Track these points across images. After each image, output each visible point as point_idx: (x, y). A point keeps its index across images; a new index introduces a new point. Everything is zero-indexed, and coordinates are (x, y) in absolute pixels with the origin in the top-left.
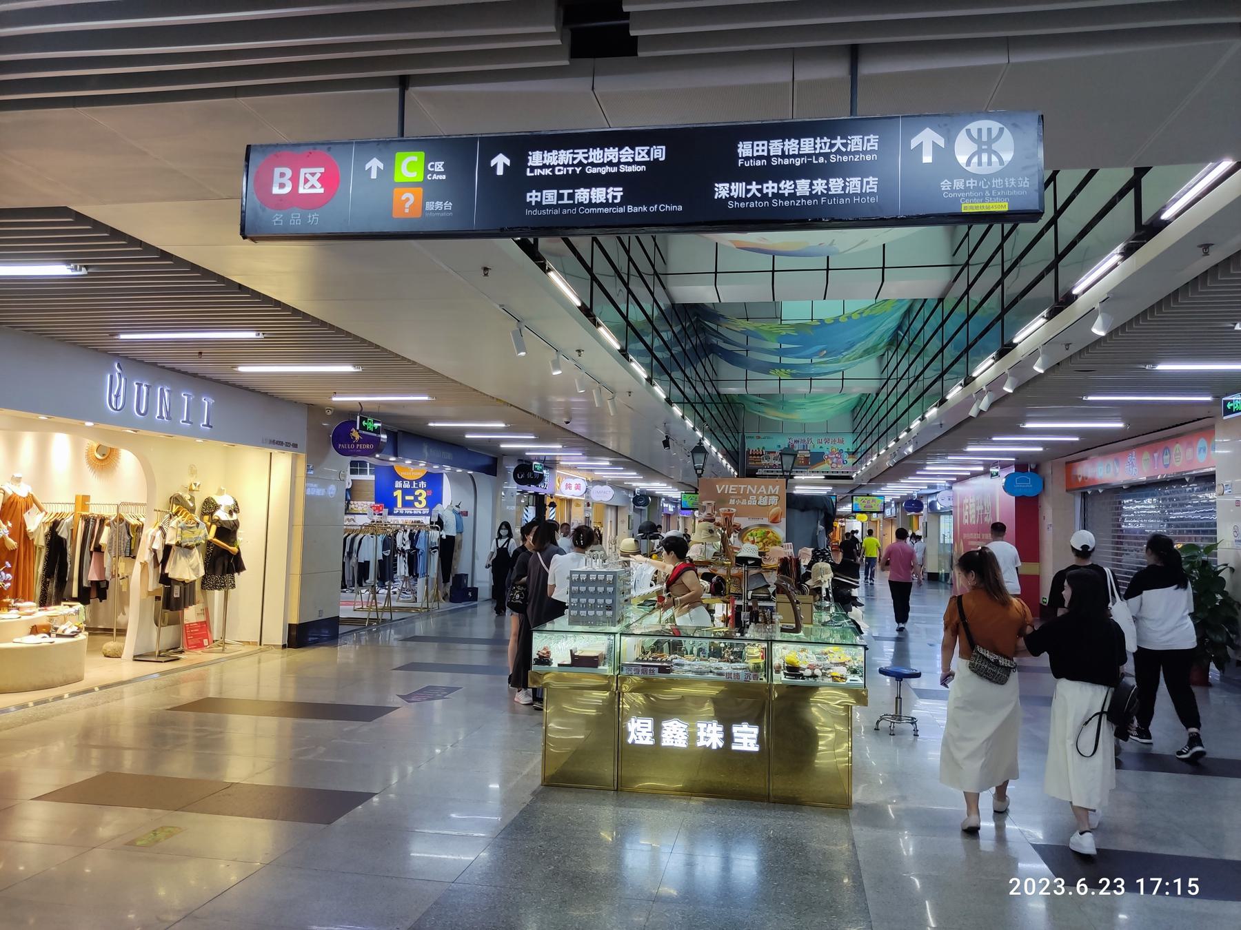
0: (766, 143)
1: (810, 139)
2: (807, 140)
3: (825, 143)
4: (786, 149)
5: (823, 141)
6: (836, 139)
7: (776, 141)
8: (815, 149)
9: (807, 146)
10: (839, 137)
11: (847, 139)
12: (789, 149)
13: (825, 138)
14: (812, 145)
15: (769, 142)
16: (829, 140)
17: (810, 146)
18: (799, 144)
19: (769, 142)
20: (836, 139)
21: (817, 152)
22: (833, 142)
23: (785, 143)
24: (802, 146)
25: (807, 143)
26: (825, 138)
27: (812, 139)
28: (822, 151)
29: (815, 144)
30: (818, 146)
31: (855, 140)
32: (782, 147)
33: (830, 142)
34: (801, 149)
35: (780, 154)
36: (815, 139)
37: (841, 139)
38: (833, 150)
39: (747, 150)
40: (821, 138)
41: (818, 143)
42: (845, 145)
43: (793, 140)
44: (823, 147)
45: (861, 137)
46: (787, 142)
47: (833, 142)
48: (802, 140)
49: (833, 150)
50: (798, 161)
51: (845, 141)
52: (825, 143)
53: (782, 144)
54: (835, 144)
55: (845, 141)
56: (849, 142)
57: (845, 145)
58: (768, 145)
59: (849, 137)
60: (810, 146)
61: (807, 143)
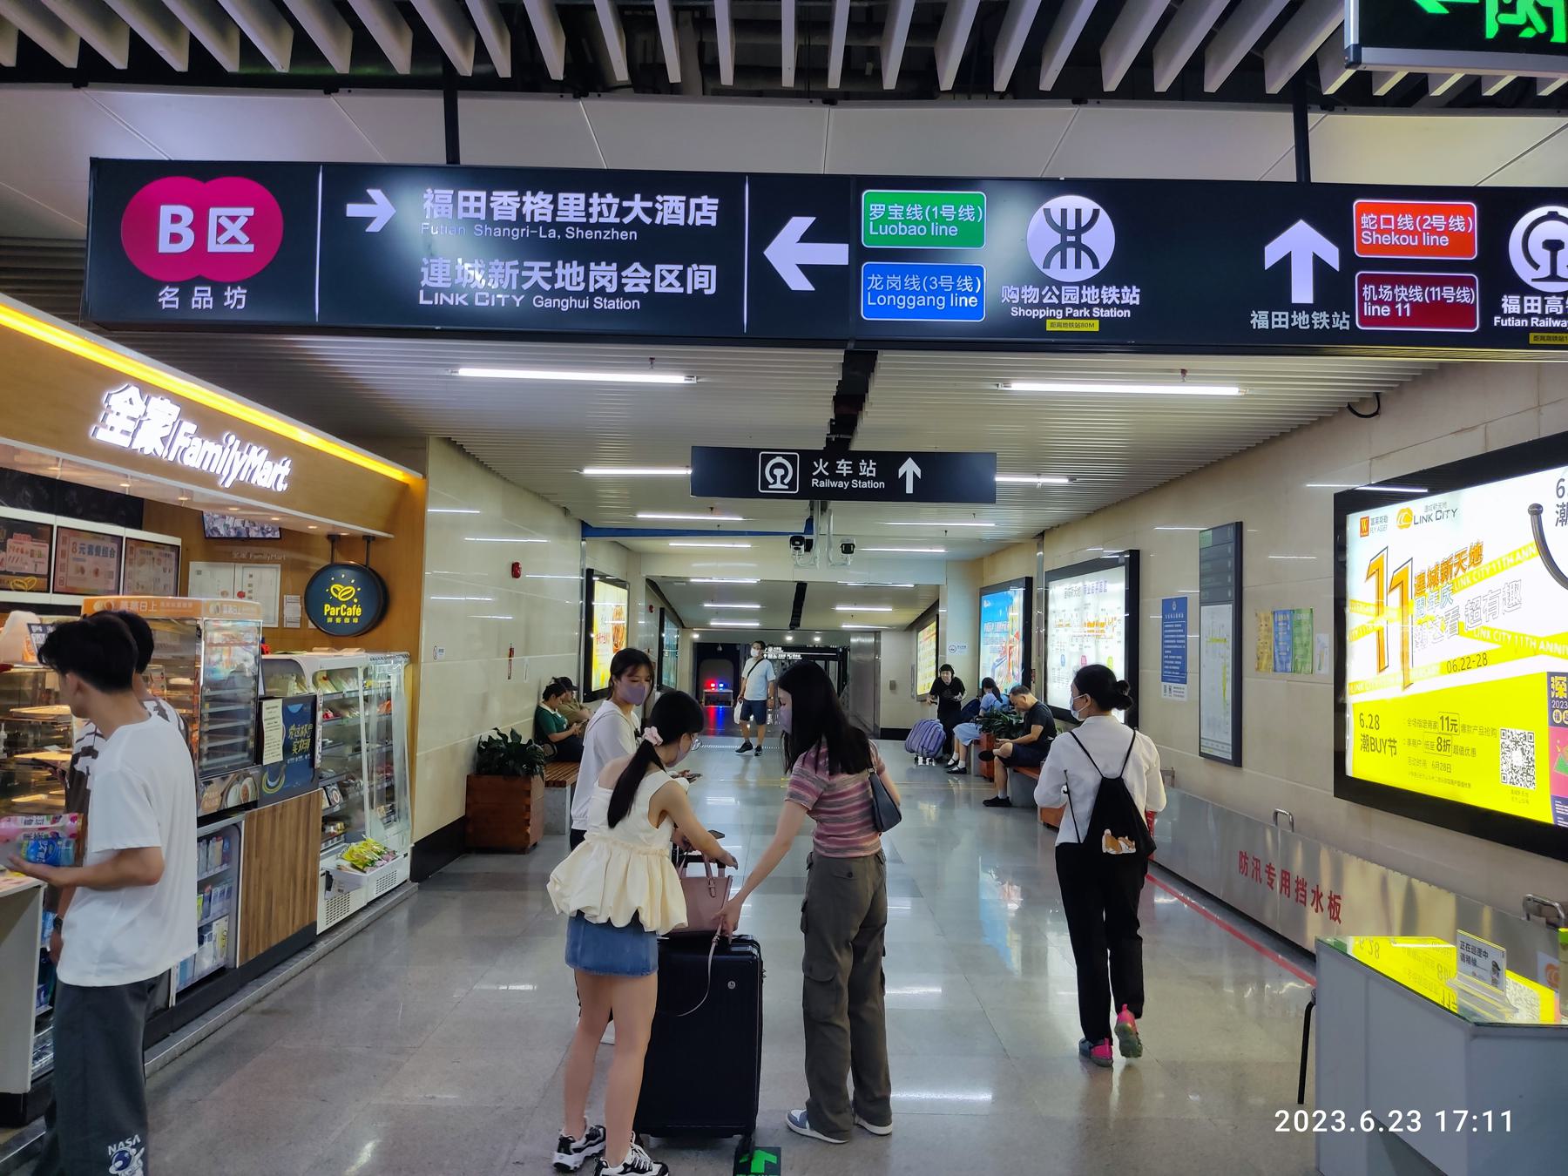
0: (483, 194)
1: (577, 195)
2: (572, 196)
3: (609, 206)
4: (527, 209)
5: (603, 200)
6: (632, 199)
7: (505, 194)
8: (589, 215)
9: (571, 208)
10: (638, 197)
11: (655, 201)
12: (533, 212)
13: (609, 196)
14: (582, 207)
15: (489, 195)
16: (617, 200)
17: (577, 208)
18: (555, 202)
19: (489, 195)
20: (632, 199)
21: (592, 221)
22: (625, 204)
23: (524, 199)
24: (561, 207)
25: (572, 202)
26: (609, 196)
27: (582, 196)
28: (601, 220)
29: (588, 205)
30: (594, 210)
31: (671, 204)
32: (519, 205)
33: (620, 204)
34: (559, 213)
35: (514, 218)
36: (588, 196)
37: (643, 199)
38: (627, 220)
39: (443, 206)
40: (602, 195)
41: (595, 205)
42: (651, 212)
43: (541, 194)
44: (606, 213)
45: (684, 198)
46: (528, 198)
47: (625, 204)
48: (561, 196)
49: (627, 220)
50: (515, 232)
51: (649, 204)
52: (609, 206)
53: (518, 199)
54: (630, 209)
55: (649, 204)
56: (658, 206)
57: (651, 212)
58: (488, 201)
59: (659, 198)
60: (577, 208)
61: (572, 202)
